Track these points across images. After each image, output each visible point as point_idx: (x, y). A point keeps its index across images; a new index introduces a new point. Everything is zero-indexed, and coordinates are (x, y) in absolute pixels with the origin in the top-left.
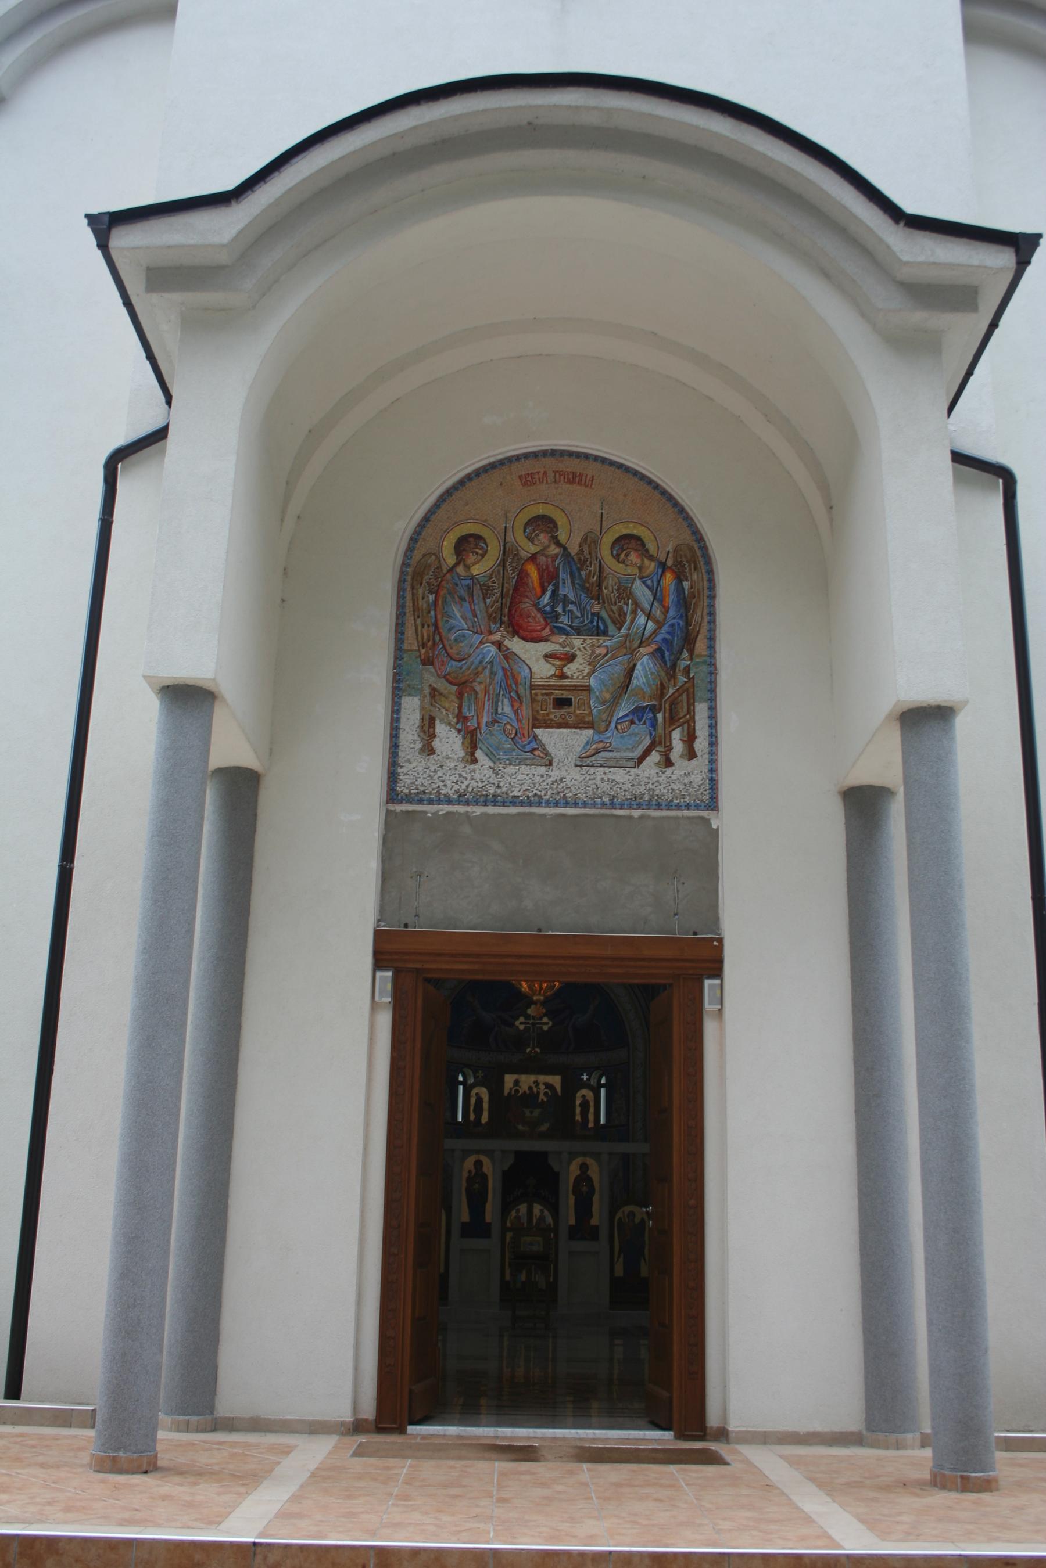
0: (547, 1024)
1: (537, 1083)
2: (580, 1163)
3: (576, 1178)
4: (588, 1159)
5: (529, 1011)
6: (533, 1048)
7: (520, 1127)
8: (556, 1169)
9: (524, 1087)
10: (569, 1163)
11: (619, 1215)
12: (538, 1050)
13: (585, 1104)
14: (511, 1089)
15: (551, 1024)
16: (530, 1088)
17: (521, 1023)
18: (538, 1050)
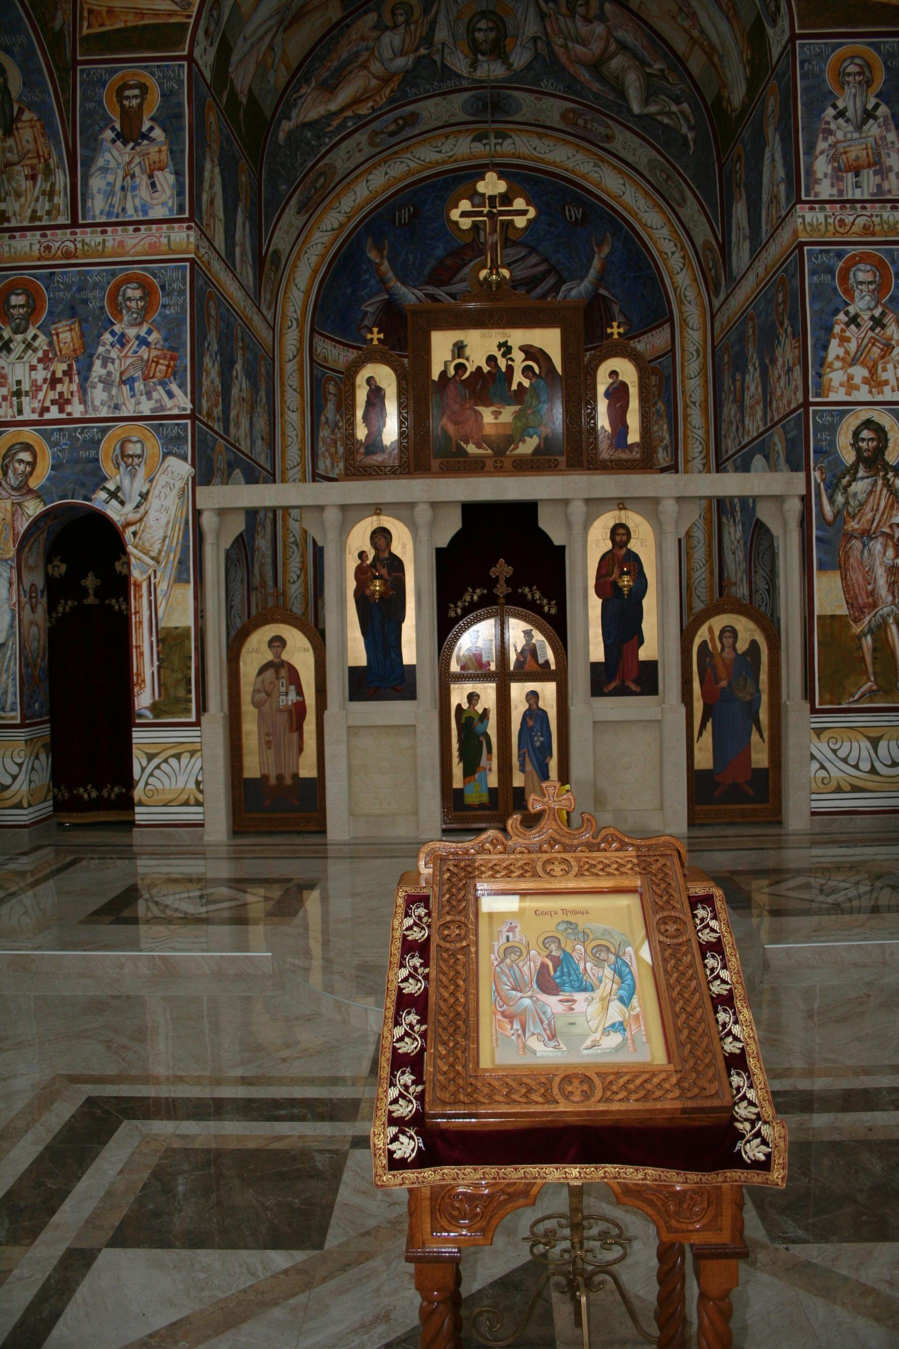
0: (524, 213)
1: (506, 349)
2: (611, 524)
4: (630, 514)
5: (481, 187)
6: (494, 267)
8: (557, 541)
9: (476, 359)
10: (587, 525)
11: (702, 634)
13: (618, 393)
14: (446, 363)
15: (532, 213)
16: (491, 359)
17: (464, 214)
18: (505, 273)
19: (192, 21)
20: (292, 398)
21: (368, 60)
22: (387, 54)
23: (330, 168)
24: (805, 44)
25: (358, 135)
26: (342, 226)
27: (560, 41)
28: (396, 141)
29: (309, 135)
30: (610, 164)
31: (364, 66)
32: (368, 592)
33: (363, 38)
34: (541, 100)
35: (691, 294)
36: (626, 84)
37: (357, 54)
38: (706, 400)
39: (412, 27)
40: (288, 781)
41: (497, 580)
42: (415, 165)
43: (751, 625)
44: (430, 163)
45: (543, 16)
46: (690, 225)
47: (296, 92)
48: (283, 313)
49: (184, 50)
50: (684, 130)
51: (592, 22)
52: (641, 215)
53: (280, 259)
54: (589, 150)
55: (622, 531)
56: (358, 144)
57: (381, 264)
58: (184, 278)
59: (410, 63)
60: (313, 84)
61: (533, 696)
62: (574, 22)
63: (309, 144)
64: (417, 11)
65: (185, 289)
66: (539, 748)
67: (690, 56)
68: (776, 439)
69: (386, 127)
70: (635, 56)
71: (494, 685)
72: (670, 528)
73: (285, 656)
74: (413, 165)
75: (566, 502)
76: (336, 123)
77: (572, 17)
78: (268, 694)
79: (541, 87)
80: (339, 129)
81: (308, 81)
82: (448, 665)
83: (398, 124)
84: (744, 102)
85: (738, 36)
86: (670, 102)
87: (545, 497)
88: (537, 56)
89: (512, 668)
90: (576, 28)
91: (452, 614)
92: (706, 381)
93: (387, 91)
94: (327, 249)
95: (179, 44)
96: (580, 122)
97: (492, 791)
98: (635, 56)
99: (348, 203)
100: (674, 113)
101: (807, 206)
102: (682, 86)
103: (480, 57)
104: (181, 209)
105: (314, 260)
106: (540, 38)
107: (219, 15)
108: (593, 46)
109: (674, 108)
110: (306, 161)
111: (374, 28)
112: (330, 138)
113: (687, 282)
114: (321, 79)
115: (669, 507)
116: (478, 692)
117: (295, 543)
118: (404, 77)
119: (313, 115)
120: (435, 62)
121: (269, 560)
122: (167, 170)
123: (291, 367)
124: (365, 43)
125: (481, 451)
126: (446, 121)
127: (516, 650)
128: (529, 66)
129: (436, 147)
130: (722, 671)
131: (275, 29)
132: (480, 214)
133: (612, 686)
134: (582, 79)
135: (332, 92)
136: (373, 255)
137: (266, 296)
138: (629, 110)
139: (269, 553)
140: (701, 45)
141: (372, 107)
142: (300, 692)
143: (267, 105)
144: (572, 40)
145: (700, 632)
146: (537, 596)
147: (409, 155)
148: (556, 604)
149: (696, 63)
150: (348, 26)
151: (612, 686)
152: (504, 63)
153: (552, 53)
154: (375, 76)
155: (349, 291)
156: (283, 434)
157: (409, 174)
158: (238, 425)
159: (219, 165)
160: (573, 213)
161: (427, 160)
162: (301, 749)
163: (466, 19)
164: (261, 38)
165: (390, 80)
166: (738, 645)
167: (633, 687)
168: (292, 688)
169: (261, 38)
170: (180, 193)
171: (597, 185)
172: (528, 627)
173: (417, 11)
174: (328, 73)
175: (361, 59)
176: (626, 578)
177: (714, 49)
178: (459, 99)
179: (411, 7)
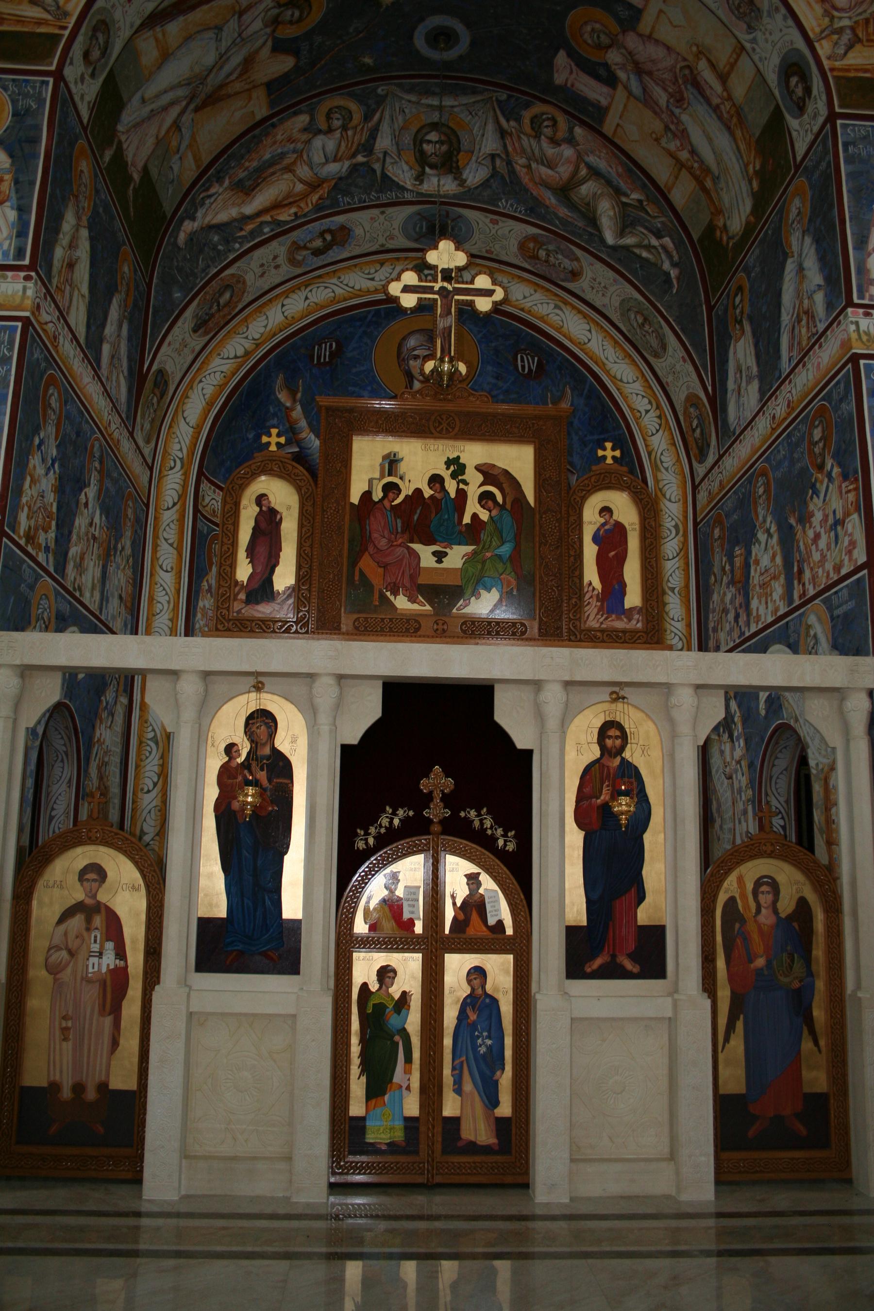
0: (489, 293)
1: (457, 467)
2: (598, 723)
3: (587, 770)
5: (432, 257)
7: (402, 602)
8: (521, 743)
11: (729, 887)
12: (462, 368)
14: (371, 481)
17: (407, 289)
19: (67, 33)
20: (167, 555)
21: (294, 163)
22: (318, 158)
23: (238, 282)
24: (848, 125)
25: (274, 244)
26: (247, 354)
27: (523, 161)
28: (320, 264)
29: (216, 238)
30: (574, 307)
31: (289, 169)
32: (236, 805)
33: (290, 140)
34: (487, 251)
35: (668, 460)
36: (599, 212)
37: (282, 156)
38: (687, 586)
39: (350, 133)
40: (91, 1095)
41: (430, 797)
42: (341, 291)
43: (799, 876)
44: (360, 290)
45: (503, 134)
46: (668, 379)
47: (204, 191)
48: (165, 451)
49: (51, 64)
50: (666, 266)
51: (560, 145)
52: (609, 366)
53: (166, 383)
54: (548, 290)
55: (613, 732)
56: (275, 257)
57: (292, 409)
58: (11, 342)
59: (344, 170)
60: (227, 183)
61: (478, 974)
62: (539, 141)
63: (215, 248)
64: (357, 117)
65: (11, 357)
66: (484, 1056)
67: (674, 183)
68: (812, 619)
69: (310, 241)
70: (609, 182)
71: (419, 956)
72: (685, 729)
73: (102, 897)
74: (339, 291)
75: (537, 685)
76: (250, 227)
77: (537, 136)
78: (71, 954)
79: (498, 206)
80: (253, 234)
81: (220, 180)
82: (351, 922)
83: (325, 239)
84: (748, 223)
85: (742, 147)
86: (650, 236)
87: (508, 676)
88: (494, 174)
89: (447, 931)
90: (541, 149)
91: (361, 845)
92: (687, 564)
93: (315, 198)
94: (227, 379)
95: (46, 56)
96: (542, 254)
97: (409, 1121)
98: (609, 182)
99: (257, 328)
100: (654, 247)
101: (861, 311)
102: (663, 219)
103: (427, 169)
104: (20, 253)
105: (209, 391)
106: (498, 155)
107: (107, 42)
108: (561, 169)
109: (654, 242)
110: (209, 266)
111: (305, 130)
112: (241, 244)
113: (664, 446)
114: (237, 179)
115: (685, 698)
116: (394, 964)
117: (155, 740)
118: (336, 184)
119: (222, 217)
120: (374, 171)
121: (116, 760)
122: (8, 204)
123: (168, 516)
124: (292, 146)
125: (416, 607)
126: (383, 245)
127: (454, 904)
128: (485, 184)
129: (369, 274)
130: (757, 943)
131: (184, 103)
132: (430, 290)
133: (598, 962)
134: (547, 203)
135: (247, 194)
136: (283, 397)
137: (143, 423)
138: (603, 241)
139: (118, 749)
140: (690, 170)
141: (296, 214)
142: (121, 953)
143: (168, 200)
144: (537, 161)
145: (725, 884)
146: (488, 823)
147: (335, 281)
148: (515, 837)
149: (680, 195)
150: (274, 126)
151: (598, 962)
152: (455, 179)
153: (512, 172)
154: (301, 181)
155: (251, 436)
156: (151, 599)
157: (334, 301)
158: (80, 568)
159: (90, 228)
160: (527, 363)
161: (357, 287)
162: (115, 1043)
163: (414, 130)
164: (165, 109)
165: (319, 186)
166: (779, 905)
167: (629, 965)
168: (110, 945)
169: (165, 109)
170: (21, 234)
171: (559, 329)
172: (473, 868)
173: (357, 117)
174: (246, 173)
175: (286, 161)
176: (624, 800)
177: (707, 170)
178: (401, 214)
179: (350, 112)
